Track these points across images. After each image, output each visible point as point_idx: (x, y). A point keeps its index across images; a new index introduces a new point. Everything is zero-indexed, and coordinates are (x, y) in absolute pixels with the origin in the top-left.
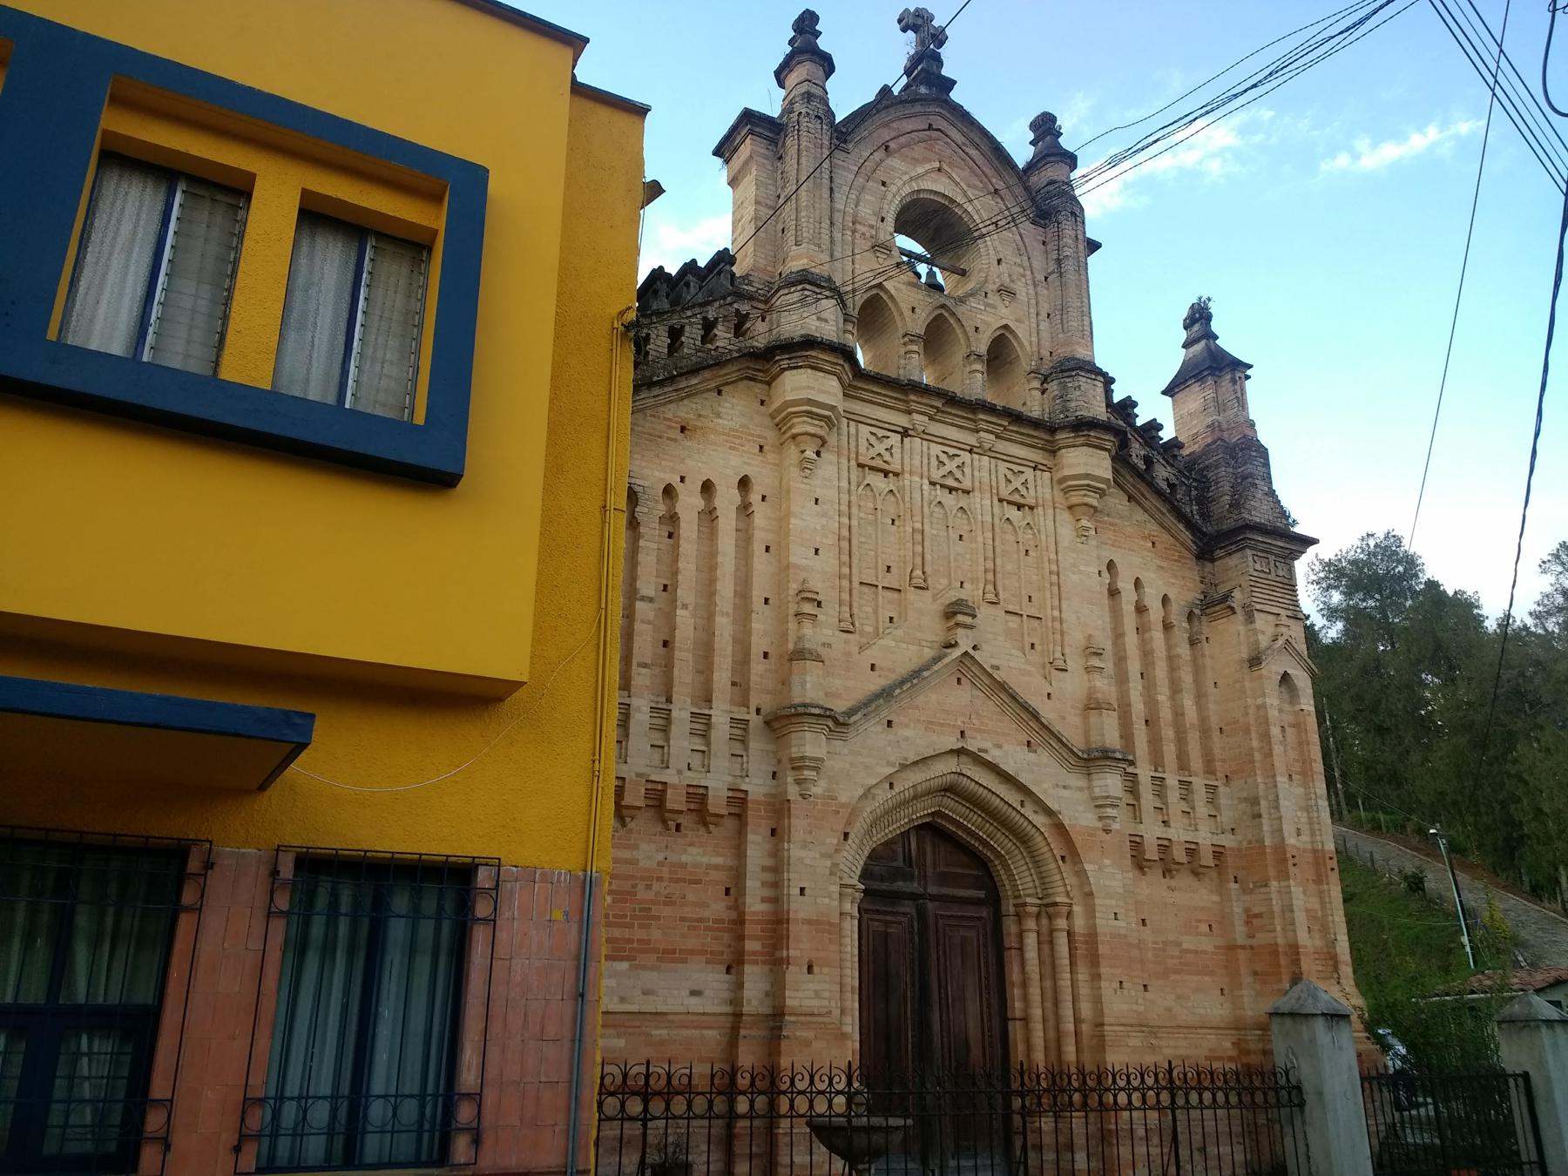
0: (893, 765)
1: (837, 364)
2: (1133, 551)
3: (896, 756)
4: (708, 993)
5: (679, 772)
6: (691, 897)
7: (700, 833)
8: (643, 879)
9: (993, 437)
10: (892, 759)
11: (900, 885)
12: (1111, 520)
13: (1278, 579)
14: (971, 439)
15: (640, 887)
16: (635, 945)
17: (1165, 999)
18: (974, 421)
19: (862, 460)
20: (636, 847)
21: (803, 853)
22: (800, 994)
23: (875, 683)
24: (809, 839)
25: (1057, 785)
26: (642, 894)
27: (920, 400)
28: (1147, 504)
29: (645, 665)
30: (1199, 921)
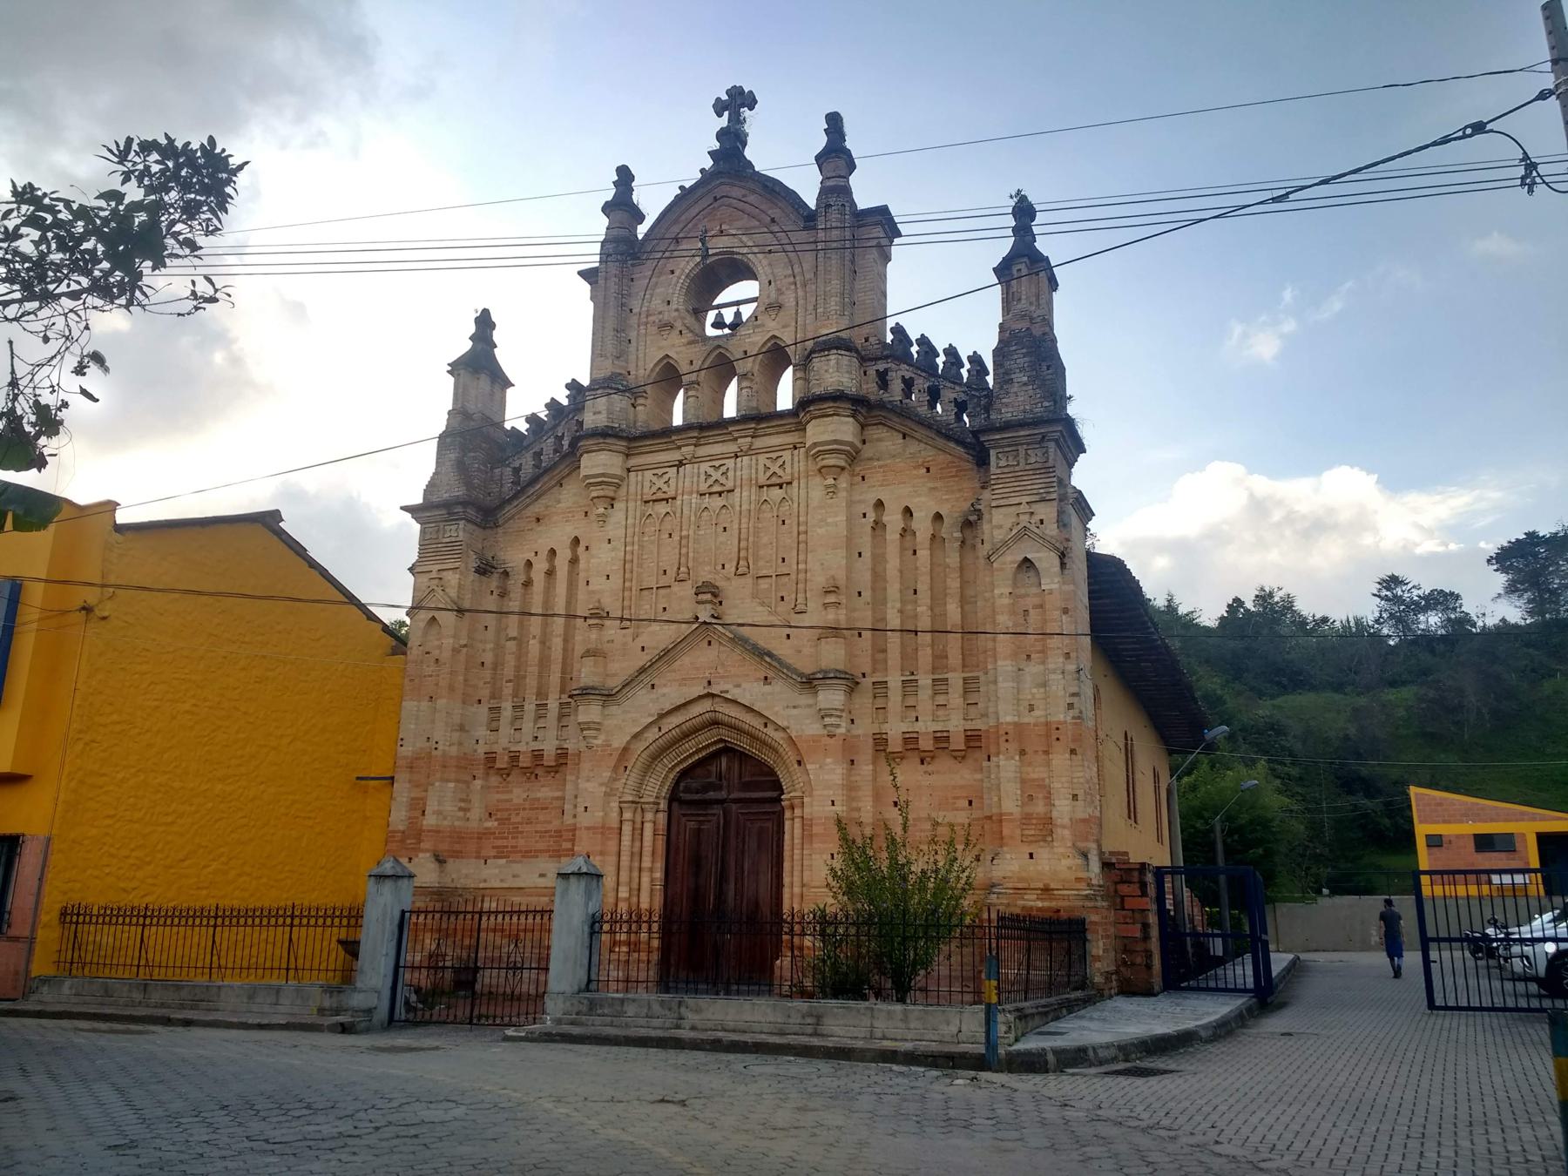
0: (653, 715)
2: (904, 483)
3: (655, 709)
5: (527, 743)
6: (541, 818)
8: (516, 810)
9: (749, 439)
10: (653, 712)
11: (712, 795)
12: (881, 463)
13: (1028, 467)
14: (733, 448)
15: (513, 816)
18: (730, 433)
19: (646, 498)
20: (511, 792)
23: (643, 659)
25: (788, 707)
26: (514, 819)
28: (917, 435)
29: (510, 681)
30: (958, 798)
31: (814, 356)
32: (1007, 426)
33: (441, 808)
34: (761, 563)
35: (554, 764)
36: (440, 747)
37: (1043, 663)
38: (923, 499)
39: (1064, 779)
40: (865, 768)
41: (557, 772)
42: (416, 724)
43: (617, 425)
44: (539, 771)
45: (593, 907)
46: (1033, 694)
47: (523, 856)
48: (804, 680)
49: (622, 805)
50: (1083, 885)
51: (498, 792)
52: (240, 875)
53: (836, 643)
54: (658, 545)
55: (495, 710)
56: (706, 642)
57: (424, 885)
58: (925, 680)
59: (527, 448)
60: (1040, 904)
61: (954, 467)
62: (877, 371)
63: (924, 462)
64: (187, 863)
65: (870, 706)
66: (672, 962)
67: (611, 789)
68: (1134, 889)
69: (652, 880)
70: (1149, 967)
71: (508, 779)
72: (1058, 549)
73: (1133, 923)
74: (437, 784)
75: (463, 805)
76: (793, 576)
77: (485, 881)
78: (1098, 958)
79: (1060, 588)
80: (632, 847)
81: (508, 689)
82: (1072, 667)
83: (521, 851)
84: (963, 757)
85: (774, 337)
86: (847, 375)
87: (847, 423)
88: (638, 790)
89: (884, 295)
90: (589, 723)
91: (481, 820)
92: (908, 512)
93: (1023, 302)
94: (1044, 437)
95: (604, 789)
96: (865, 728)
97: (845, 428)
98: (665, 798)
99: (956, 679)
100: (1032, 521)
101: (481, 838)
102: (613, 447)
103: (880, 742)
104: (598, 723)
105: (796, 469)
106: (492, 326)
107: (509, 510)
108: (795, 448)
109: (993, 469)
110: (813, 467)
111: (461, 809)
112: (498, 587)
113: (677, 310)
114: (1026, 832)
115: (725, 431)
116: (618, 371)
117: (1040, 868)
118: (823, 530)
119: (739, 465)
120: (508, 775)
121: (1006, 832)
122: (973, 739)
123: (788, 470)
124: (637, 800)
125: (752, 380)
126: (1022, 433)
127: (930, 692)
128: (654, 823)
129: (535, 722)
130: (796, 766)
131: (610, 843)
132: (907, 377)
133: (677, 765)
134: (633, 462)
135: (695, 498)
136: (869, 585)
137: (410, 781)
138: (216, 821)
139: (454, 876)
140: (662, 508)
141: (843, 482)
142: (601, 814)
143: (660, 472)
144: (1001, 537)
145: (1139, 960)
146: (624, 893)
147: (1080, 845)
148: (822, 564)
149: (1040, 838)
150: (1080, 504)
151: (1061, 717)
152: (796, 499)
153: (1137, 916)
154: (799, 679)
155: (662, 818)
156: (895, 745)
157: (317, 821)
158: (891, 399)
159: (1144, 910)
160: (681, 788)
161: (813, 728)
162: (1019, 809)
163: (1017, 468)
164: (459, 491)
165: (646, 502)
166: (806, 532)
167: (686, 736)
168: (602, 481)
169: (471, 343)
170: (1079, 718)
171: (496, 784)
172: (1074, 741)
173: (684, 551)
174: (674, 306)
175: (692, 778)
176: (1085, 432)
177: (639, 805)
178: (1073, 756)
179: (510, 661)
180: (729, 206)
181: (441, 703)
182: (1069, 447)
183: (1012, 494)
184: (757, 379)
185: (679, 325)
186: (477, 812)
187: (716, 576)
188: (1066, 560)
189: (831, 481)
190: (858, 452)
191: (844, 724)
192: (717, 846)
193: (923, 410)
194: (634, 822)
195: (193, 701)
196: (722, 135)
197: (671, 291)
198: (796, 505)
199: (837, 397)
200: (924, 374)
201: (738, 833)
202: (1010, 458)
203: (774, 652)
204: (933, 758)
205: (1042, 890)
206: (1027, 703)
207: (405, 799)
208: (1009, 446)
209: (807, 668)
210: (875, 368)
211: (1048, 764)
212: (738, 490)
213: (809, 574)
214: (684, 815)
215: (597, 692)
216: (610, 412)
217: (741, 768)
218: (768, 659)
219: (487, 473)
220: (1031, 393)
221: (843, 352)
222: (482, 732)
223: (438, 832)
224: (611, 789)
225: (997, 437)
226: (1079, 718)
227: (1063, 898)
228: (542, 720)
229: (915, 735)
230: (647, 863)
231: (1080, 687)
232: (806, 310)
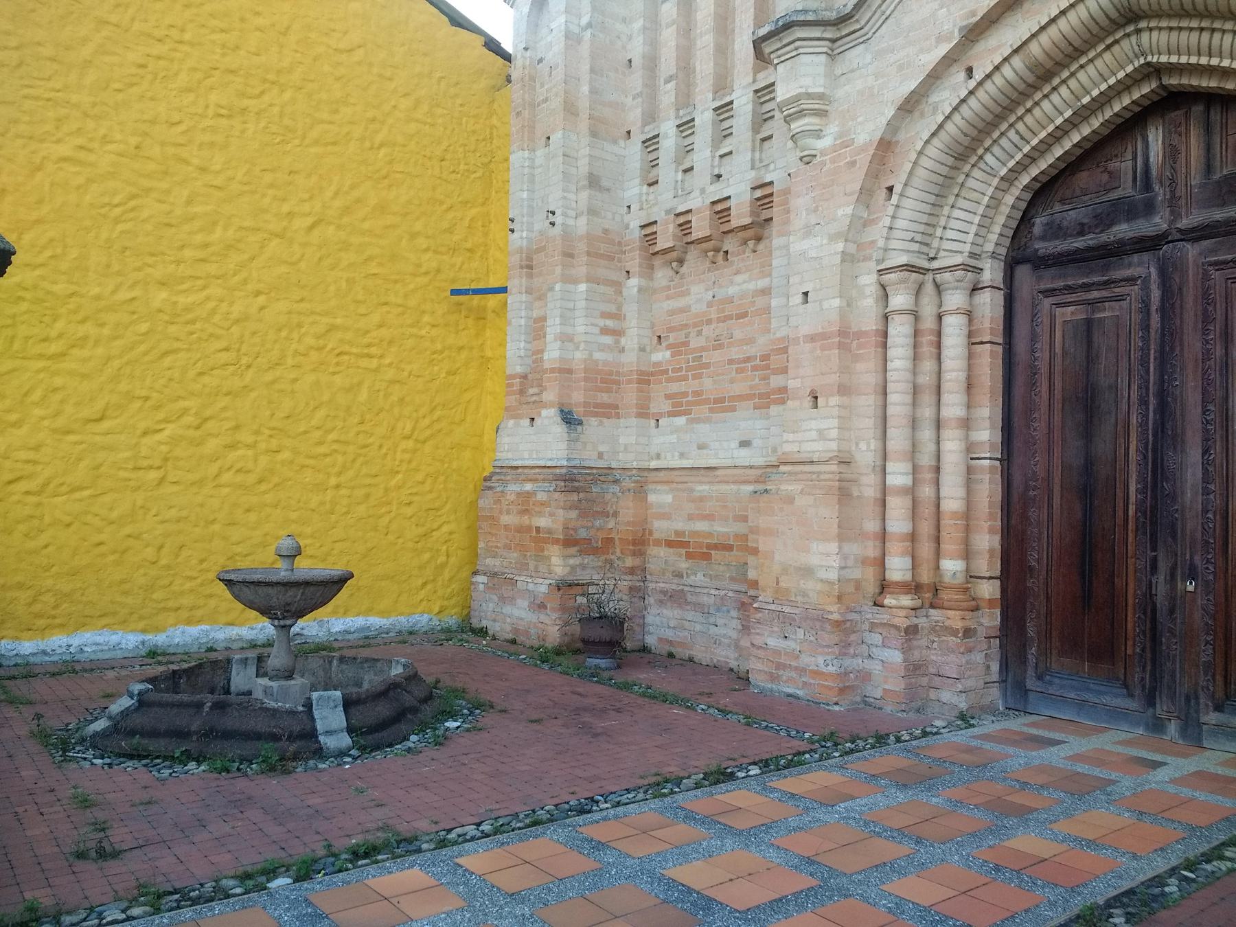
0: (948, 39)
4: (757, 442)
5: (703, 191)
6: (738, 334)
7: (747, 254)
8: (695, 325)
11: (1123, 230)
16: (690, 398)
21: (805, 245)
22: (799, 436)
24: (813, 220)
26: (695, 342)
33: (569, 330)
35: (747, 221)
36: (558, 219)
41: (759, 239)
42: (530, 191)
44: (730, 244)
47: (711, 410)
49: (887, 278)
51: (668, 298)
52: (232, 446)
55: (651, 143)
57: (549, 464)
64: (106, 425)
66: (1031, 632)
67: (860, 247)
69: (970, 448)
71: (684, 270)
74: (558, 287)
75: (610, 323)
77: (658, 456)
81: (667, 95)
83: (707, 401)
88: (925, 239)
90: (797, 99)
91: (642, 350)
95: (840, 246)
98: (994, 255)
101: (648, 382)
104: (821, 97)
111: (605, 331)
120: (681, 262)
124: (925, 264)
128: (969, 314)
129: (716, 145)
131: (860, 366)
133: (1021, 167)
137: (529, 291)
138: (166, 353)
139: (602, 448)
142: (836, 302)
146: (898, 476)
155: (990, 305)
157: (387, 361)
160: (1037, 229)
171: (664, 283)
175: (1062, 201)
177: (929, 277)
186: (631, 341)
192: (1144, 362)
194: (916, 315)
195: (80, 141)
201: (1207, 319)
207: (523, 322)
214: (1048, 293)
217: (1208, 148)
222: (634, 189)
223: (570, 371)
224: (860, 247)
228: (729, 140)
230: (953, 406)
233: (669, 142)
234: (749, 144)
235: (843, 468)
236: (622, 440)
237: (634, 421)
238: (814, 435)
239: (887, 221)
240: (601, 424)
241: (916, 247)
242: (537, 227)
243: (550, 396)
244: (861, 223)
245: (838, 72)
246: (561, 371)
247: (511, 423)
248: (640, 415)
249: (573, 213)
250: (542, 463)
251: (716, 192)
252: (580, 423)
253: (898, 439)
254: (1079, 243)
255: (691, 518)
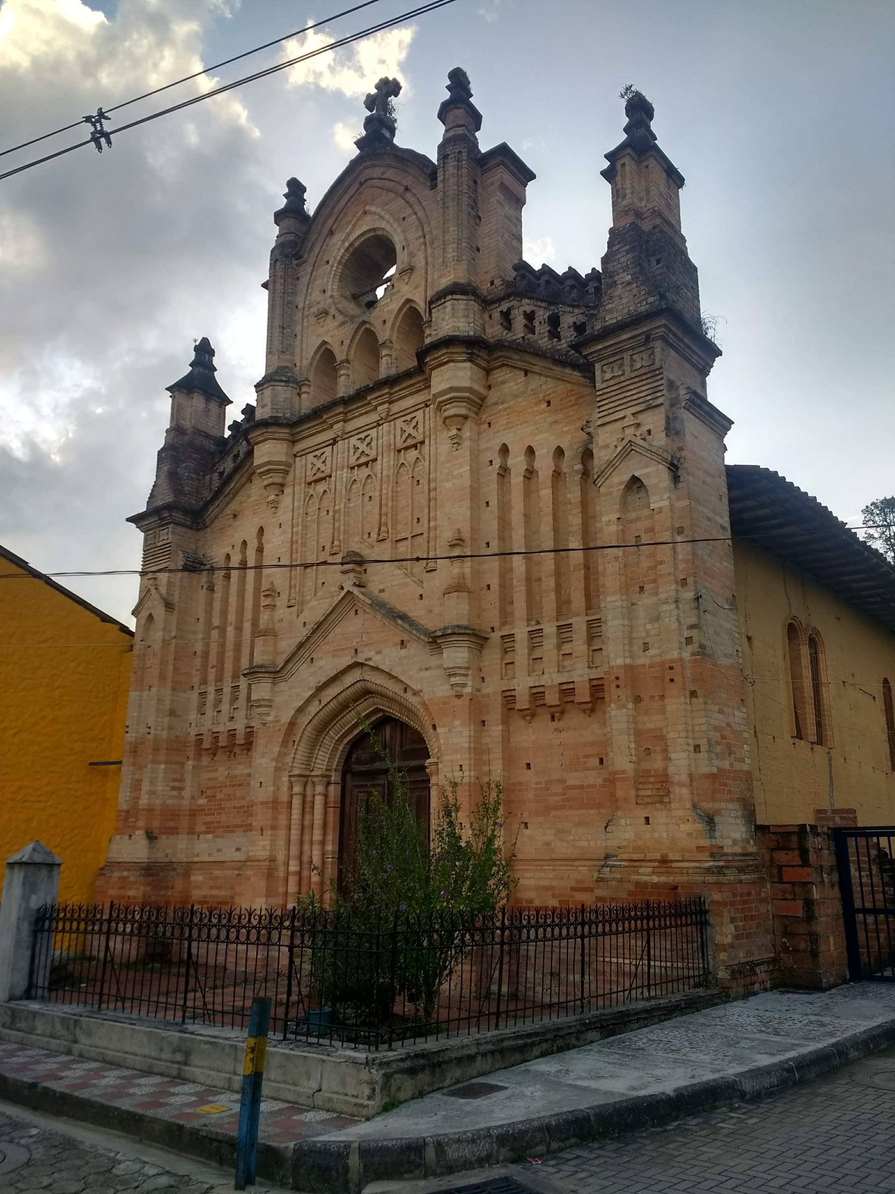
1: (263, 434)
4: (243, 849)
5: (225, 724)
6: (238, 795)
8: (219, 787)
13: (633, 375)
14: (374, 417)
17: (544, 834)
19: (309, 479)
25: (421, 670)
27: (330, 415)
29: (213, 667)
30: (588, 756)
31: (432, 306)
32: (608, 332)
34: (400, 527)
36: (152, 731)
37: (656, 594)
38: (545, 435)
39: (680, 727)
40: (494, 728)
43: (281, 415)
45: (35, 902)
46: (647, 631)
47: (224, 832)
48: (431, 640)
49: (293, 779)
50: (705, 856)
51: (208, 771)
53: (458, 597)
54: (318, 524)
55: (203, 694)
56: (353, 611)
58: (549, 629)
59: (228, 453)
60: (655, 879)
61: (574, 395)
62: (501, 312)
63: (544, 396)
65: (499, 661)
68: (793, 857)
69: (323, 854)
70: (814, 954)
71: (215, 758)
72: (665, 460)
73: (794, 900)
74: (149, 766)
75: (176, 784)
76: (425, 535)
77: (198, 855)
78: (723, 948)
79: (671, 505)
80: (303, 819)
81: (212, 674)
82: (689, 595)
84: (592, 710)
85: (408, 301)
86: (462, 320)
87: (465, 368)
88: (308, 763)
89: (519, 239)
91: (193, 798)
92: (530, 451)
93: (628, 197)
94: (648, 337)
95: (274, 764)
96: (494, 686)
97: (460, 374)
98: (336, 770)
99: (579, 623)
100: (638, 433)
101: (195, 815)
102: (276, 436)
103: (509, 698)
104: (268, 700)
105: (427, 427)
106: (212, 353)
107: (213, 510)
108: (427, 406)
109: (599, 385)
110: (440, 421)
111: (173, 788)
112: (206, 582)
113: (332, 296)
114: (642, 793)
115: (366, 402)
116: (283, 364)
117: (656, 835)
118: (450, 483)
119: (380, 433)
120: (214, 755)
121: (620, 793)
122: (597, 689)
123: (421, 430)
124: (308, 773)
125: (391, 348)
126: (625, 337)
127: (554, 641)
130: (431, 730)
132: (528, 312)
134: (299, 447)
135: (345, 473)
136: (496, 534)
137: (134, 765)
139: (168, 851)
140: (321, 487)
141: (467, 432)
142: (272, 788)
143: (318, 453)
144: (606, 458)
145: (802, 946)
146: (293, 867)
147: (705, 805)
148: (450, 518)
149: (656, 799)
150: (699, 407)
151: (675, 654)
152: (427, 457)
153: (798, 890)
154: (426, 639)
155: (334, 791)
156: (523, 702)
157: (49, 804)
158: (514, 338)
159: (806, 884)
160: (353, 759)
161: (443, 690)
162: (632, 765)
163: (622, 379)
164: (167, 498)
165: (310, 484)
166: (435, 489)
167: (344, 707)
168: (271, 468)
169: (191, 368)
170: (698, 653)
171: (207, 764)
172: (694, 681)
173: (337, 525)
174: (329, 293)
176: (717, 334)
177: (310, 779)
178: (694, 699)
179: (214, 649)
180: (372, 187)
181: (154, 690)
182: (689, 347)
183: (618, 409)
184: (396, 346)
185: (332, 311)
186: (187, 793)
187: (363, 546)
188: (680, 472)
189: (454, 432)
190: (483, 399)
191: (470, 683)
193: (543, 341)
196: (368, 122)
197: (326, 280)
198: (427, 463)
199: (449, 342)
200: (544, 305)
202: (616, 368)
203: (410, 615)
204: (562, 713)
205: (659, 861)
206: (641, 641)
207: (129, 781)
208: (613, 355)
209: (433, 623)
210: (499, 310)
211: (663, 711)
212: (379, 458)
213: (438, 532)
214: (356, 787)
215: (263, 670)
216: (274, 403)
218: (400, 622)
219: (199, 480)
220: (635, 291)
221: (458, 297)
222: (193, 716)
223: (153, 810)
225: (600, 347)
226: (698, 653)
227: (682, 871)
228: (237, 702)
229: (541, 690)
231: (699, 617)
232: (434, 266)
233: (211, 697)
234: (245, 707)
235: (271, 863)
236: (179, 846)
237: (185, 837)
238: (261, 848)
239: (292, 755)
240: (168, 838)
241: (304, 766)
242: (141, 731)
243: (141, 823)
244: (282, 755)
245: (277, 690)
246: (148, 810)
247: (118, 837)
248: (188, 833)
249: (160, 728)
250: (134, 860)
251: (231, 726)
252: (156, 838)
253: (294, 850)
254: (364, 768)
255: (211, 888)
